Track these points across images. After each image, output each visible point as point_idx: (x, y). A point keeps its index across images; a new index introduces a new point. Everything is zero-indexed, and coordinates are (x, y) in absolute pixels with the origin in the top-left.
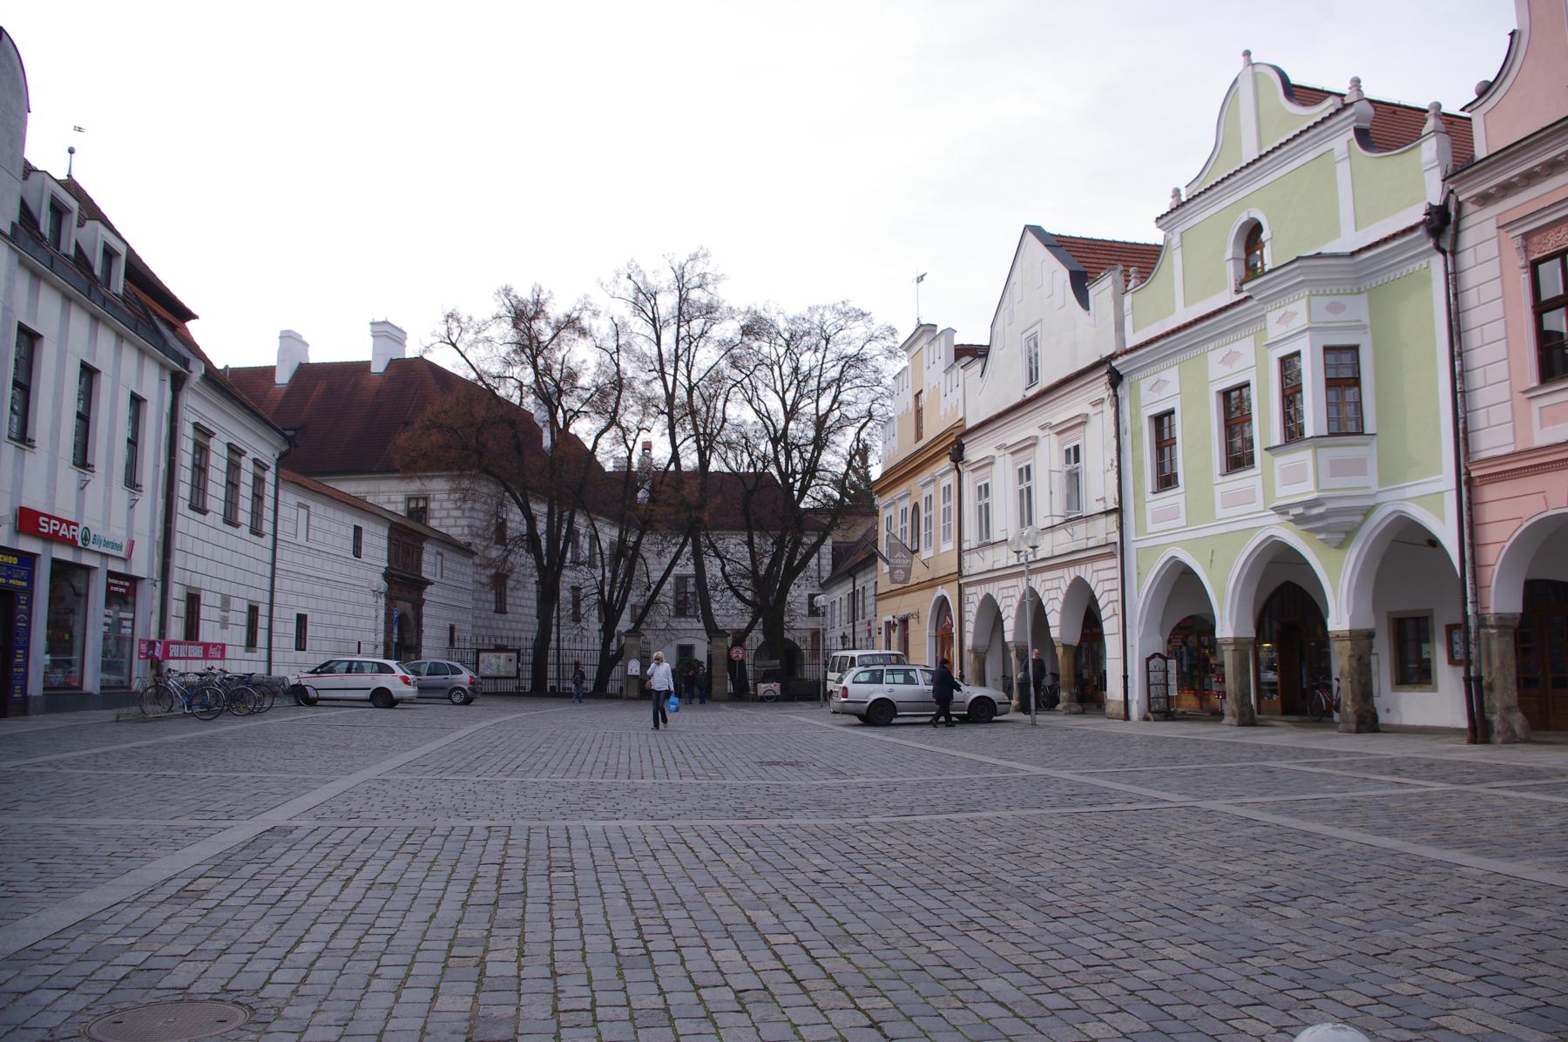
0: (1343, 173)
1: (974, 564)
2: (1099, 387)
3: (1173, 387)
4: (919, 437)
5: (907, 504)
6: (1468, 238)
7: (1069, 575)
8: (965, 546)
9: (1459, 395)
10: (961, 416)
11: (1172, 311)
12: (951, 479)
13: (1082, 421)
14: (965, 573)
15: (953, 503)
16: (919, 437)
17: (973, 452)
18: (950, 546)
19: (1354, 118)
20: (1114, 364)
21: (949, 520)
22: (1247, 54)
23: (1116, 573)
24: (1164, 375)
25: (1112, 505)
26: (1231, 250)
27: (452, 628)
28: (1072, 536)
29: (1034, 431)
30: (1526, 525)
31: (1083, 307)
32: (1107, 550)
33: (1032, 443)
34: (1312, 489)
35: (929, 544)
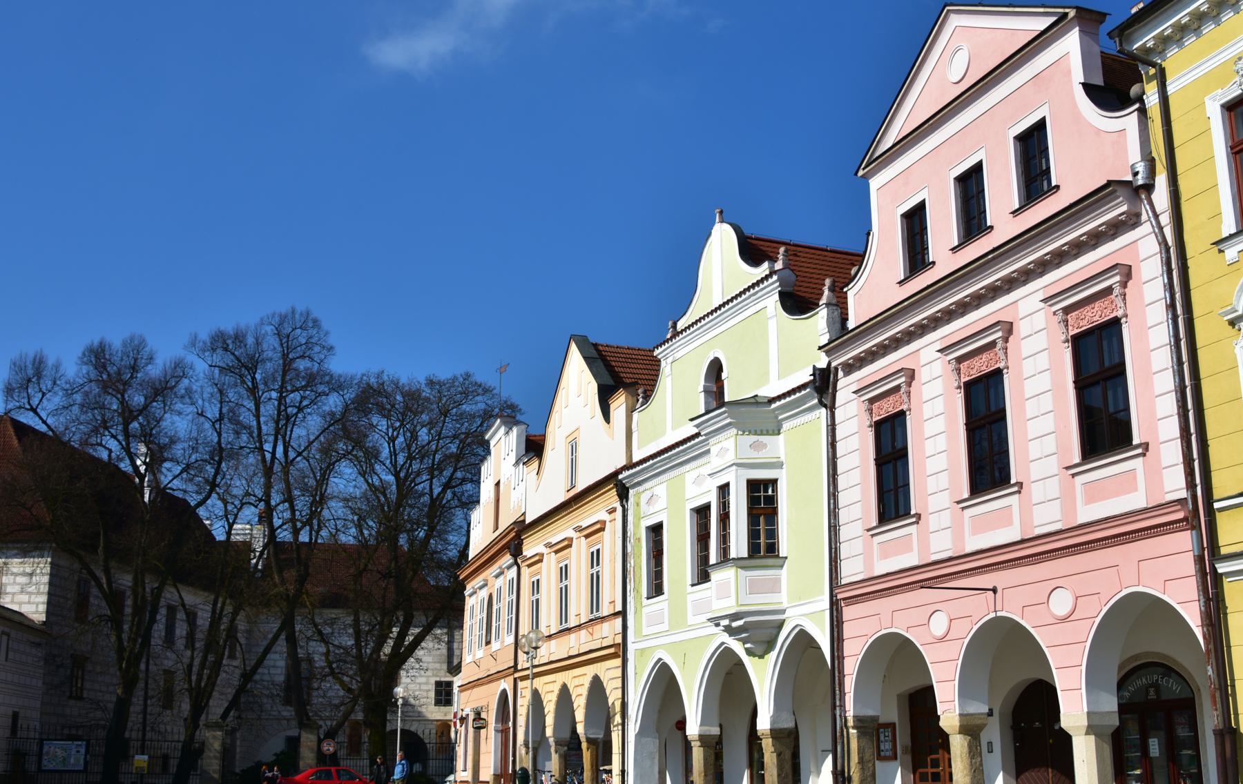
2: (611, 498)
3: (661, 503)
6: (841, 397)
7: (590, 671)
9: (832, 528)
13: (600, 527)
14: (519, 668)
15: (514, 597)
16: (496, 528)
17: (531, 547)
18: (510, 640)
19: (778, 284)
21: (512, 614)
23: (619, 672)
24: (657, 490)
25: (619, 608)
27: (15, 716)
28: (592, 635)
29: (570, 533)
30: (870, 641)
31: (605, 420)
32: (612, 650)
33: (567, 544)
34: (734, 604)
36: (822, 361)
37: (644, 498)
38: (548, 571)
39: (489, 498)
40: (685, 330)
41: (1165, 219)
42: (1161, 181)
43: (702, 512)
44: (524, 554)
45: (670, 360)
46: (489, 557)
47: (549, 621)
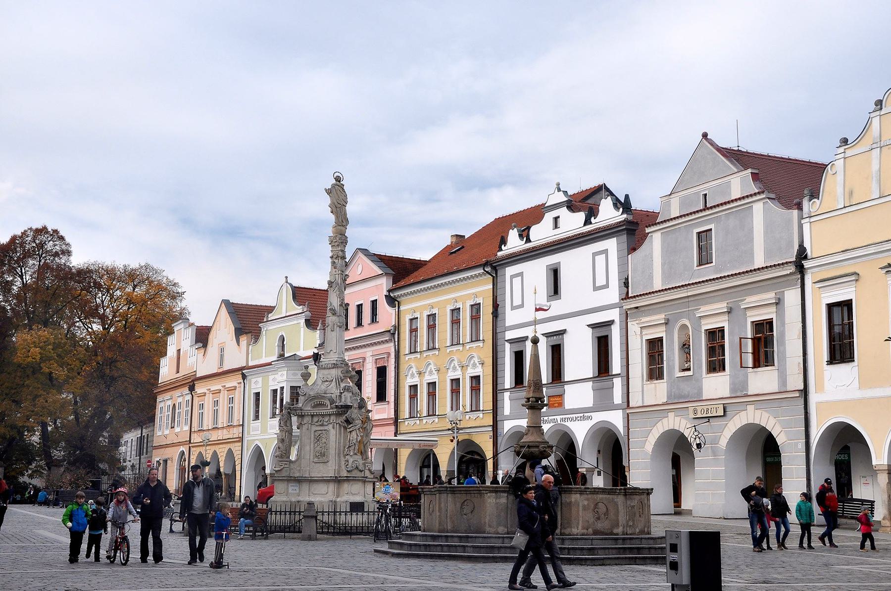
0: (302, 329)
1: (196, 438)
3: (260, 385)
4: (178, 372)
5: (170, 403)
7: (228, 447)
8: (193, 430)
10: (195, 370)
11: (262, 357)
12: (189, 397)
13: (235, 388)
16: (178, 372)
17: (200, 389)
18: (187, 428)
20: (243, 372)
22: (287, 277)
26: (277, 343)
32: (238, 439)
33: (219, 391)
35: (178, 425)
36: (316, 351)
37: (253, 380)
38: (208, 401)
39: (173, 355)
40: (270, 321)
41: (397, 344)
42: (397, 332)
43: (275, 391)
44: (196, 390)
45: (265, 329)
46: (174, 386)
47: (208, 423)
